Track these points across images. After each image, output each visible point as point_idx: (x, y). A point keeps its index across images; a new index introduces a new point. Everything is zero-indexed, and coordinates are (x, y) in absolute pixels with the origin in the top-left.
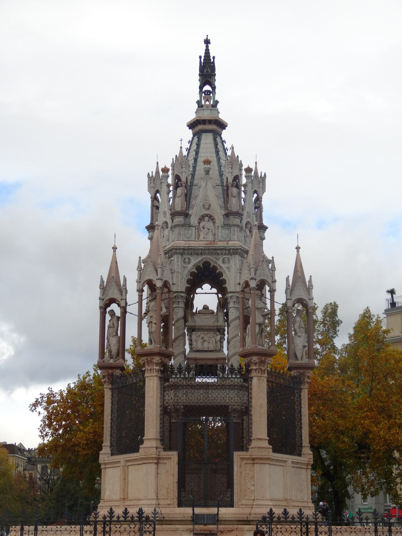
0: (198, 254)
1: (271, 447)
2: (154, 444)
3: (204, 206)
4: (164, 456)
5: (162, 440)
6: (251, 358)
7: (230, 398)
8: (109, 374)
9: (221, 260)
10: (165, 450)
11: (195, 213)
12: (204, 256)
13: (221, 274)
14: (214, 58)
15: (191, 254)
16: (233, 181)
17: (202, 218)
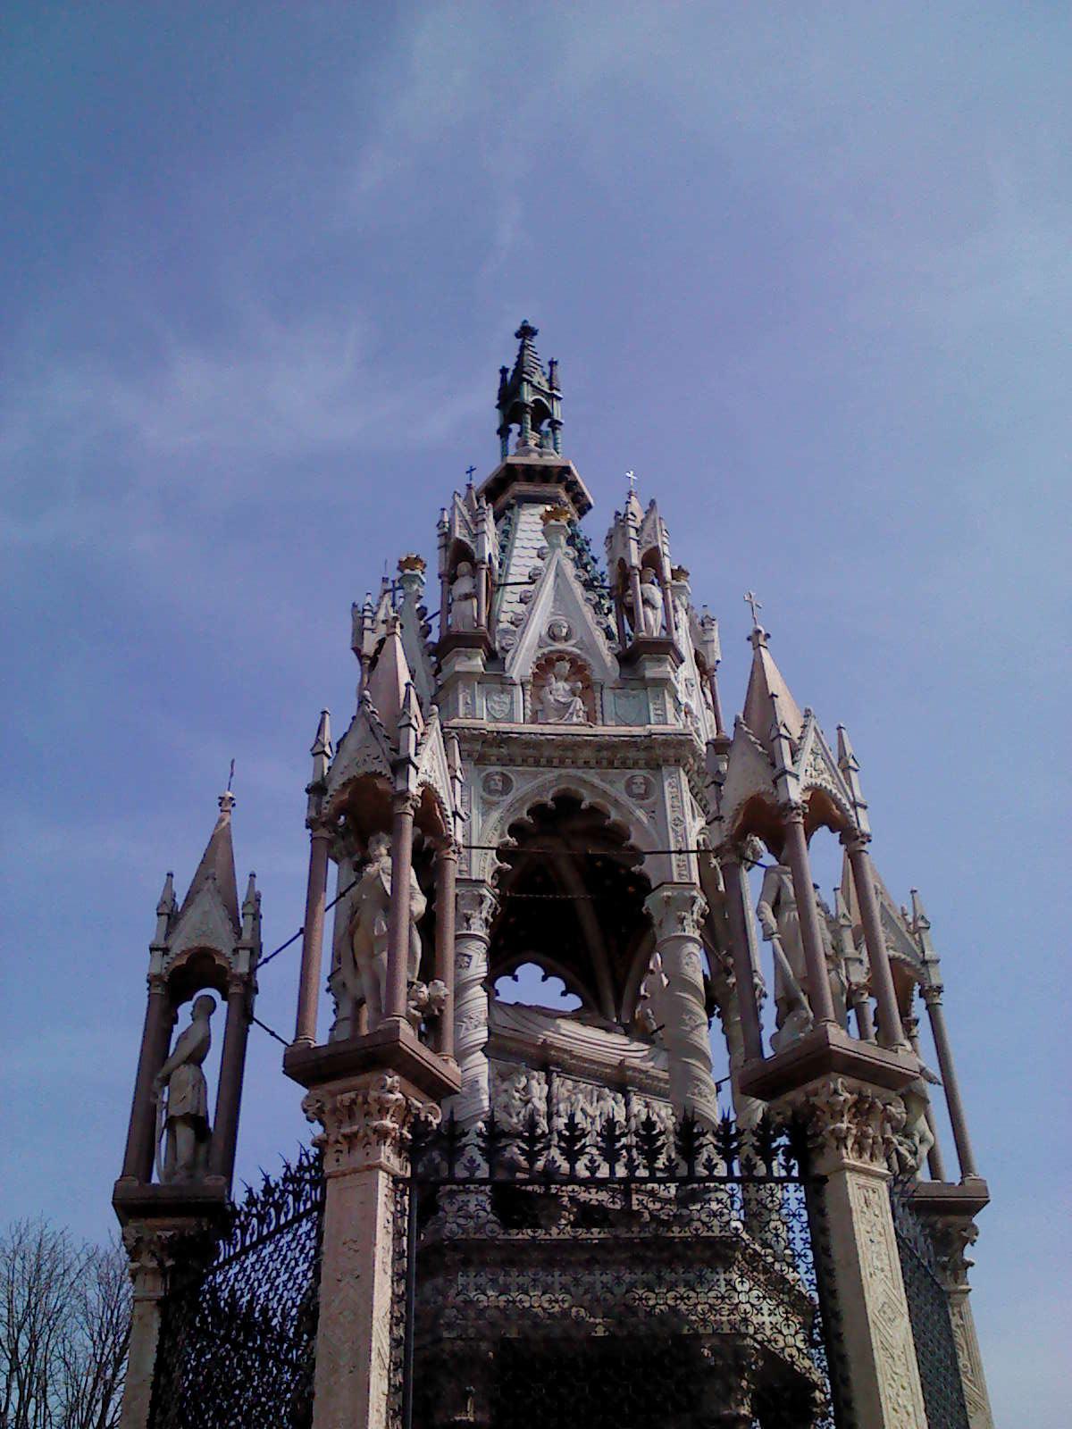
9: (621, 785)
15: (511, 761)
17: (545, 665)
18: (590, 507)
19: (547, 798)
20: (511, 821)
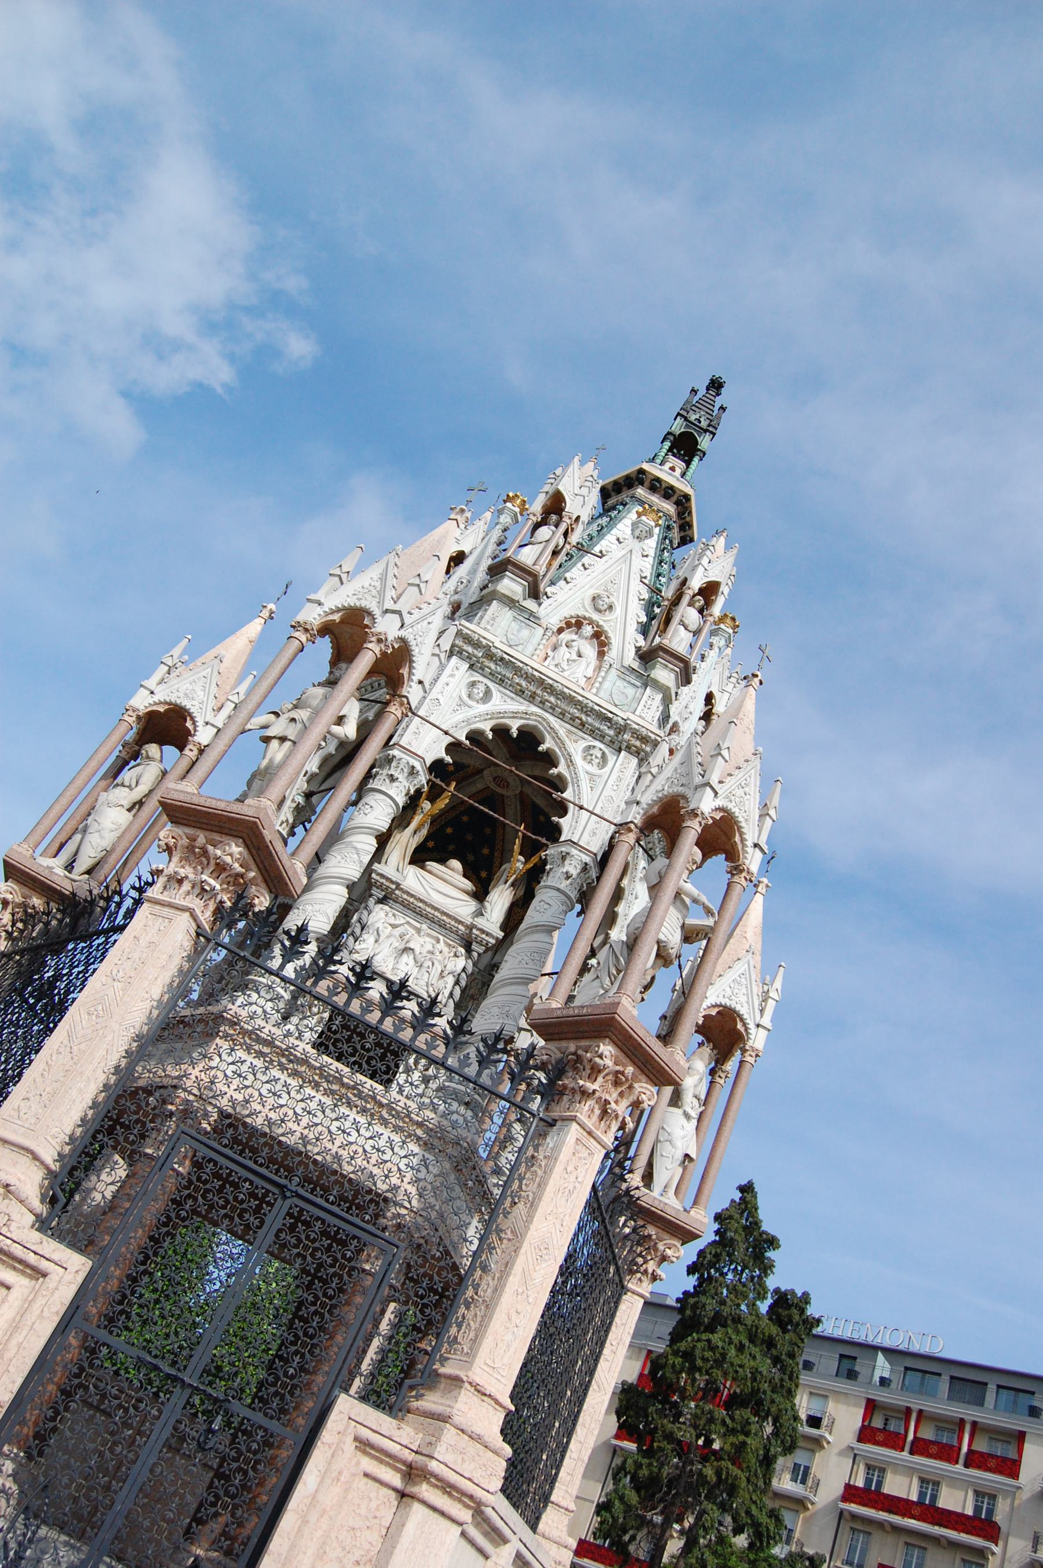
0: (521, 693)
1: (508, 1451)
3: (594, 598)
4: (18, 1251)
6: (584, 1043)
8: (24, 906)
9: (583, 744)
10: (42, 1225)
11: (564, 600)
14: (723, 409)
15: (501, 682)
17: (576, 624)
18: (692, 540)
19: (515, 726)
20: (473, 727)
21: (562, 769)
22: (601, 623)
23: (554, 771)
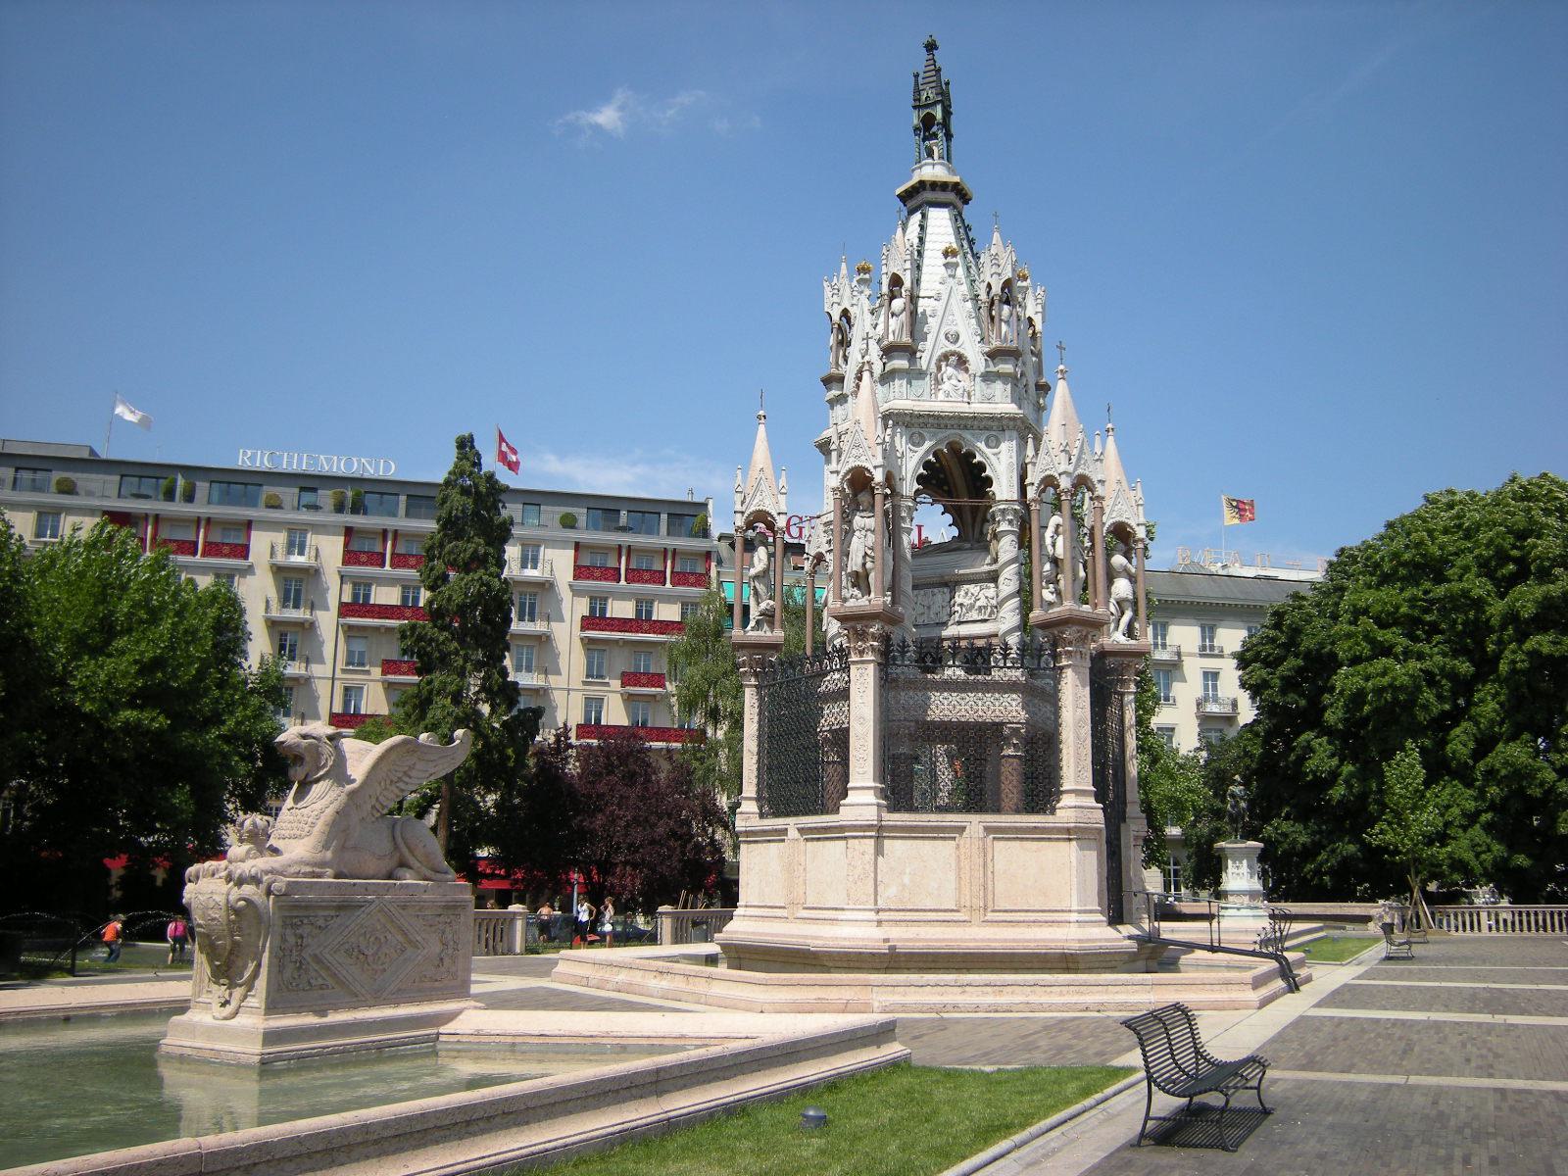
0: (939, 427)
1: (1101, 805)
2: (870, 797)
5: (882, 793)
7: (1010, 709)
11: (929, 352)
12: (949, 432)
13: (982, 467)
16: (1003, 289)
21: (979, 458)
22: (958, 350)
23: (975, 461)
